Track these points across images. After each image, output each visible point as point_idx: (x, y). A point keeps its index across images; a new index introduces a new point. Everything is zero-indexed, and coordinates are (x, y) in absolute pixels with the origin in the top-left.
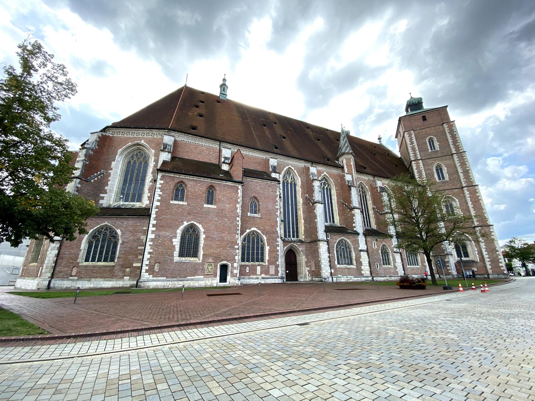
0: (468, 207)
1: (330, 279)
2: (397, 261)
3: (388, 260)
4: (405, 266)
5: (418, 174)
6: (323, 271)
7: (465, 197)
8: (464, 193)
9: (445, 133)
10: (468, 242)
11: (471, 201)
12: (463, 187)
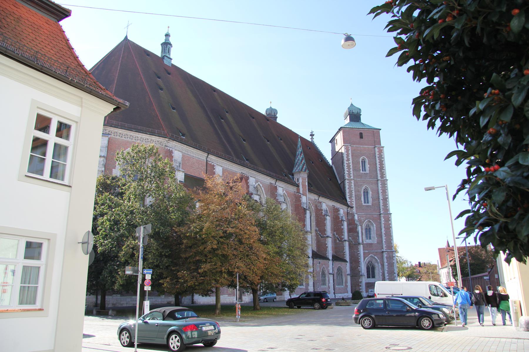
0: (381, 233)
2: (330, 281)
3: (325, 281)
4: (335, 286)
5: (349, 194)
7: (380, 223)
8: (380, 220)
9: (376, 156)
10: (376, 265)
11: (384, 227)
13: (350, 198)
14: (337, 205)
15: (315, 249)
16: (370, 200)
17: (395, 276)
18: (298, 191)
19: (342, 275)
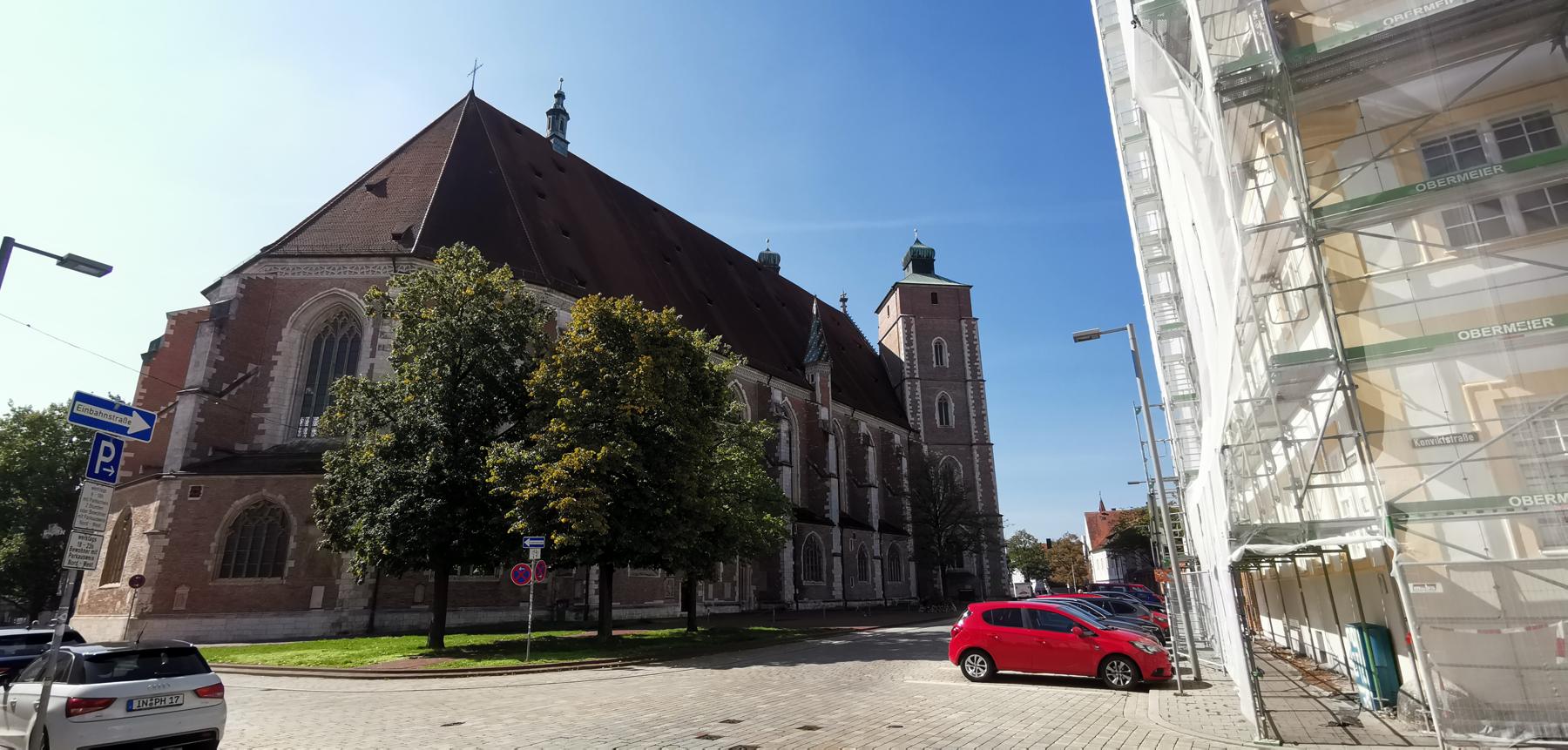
1: (795, 605)
6: (786, 592)
7: (972, 462)
11: (980, 470)
12: (972, 445)
13: (914, 414)
14: (889, 427)
15: (846, 510)
16: (952, 418)
17: (1003, 564)
18: (813, 396)
19: (898, 560)
